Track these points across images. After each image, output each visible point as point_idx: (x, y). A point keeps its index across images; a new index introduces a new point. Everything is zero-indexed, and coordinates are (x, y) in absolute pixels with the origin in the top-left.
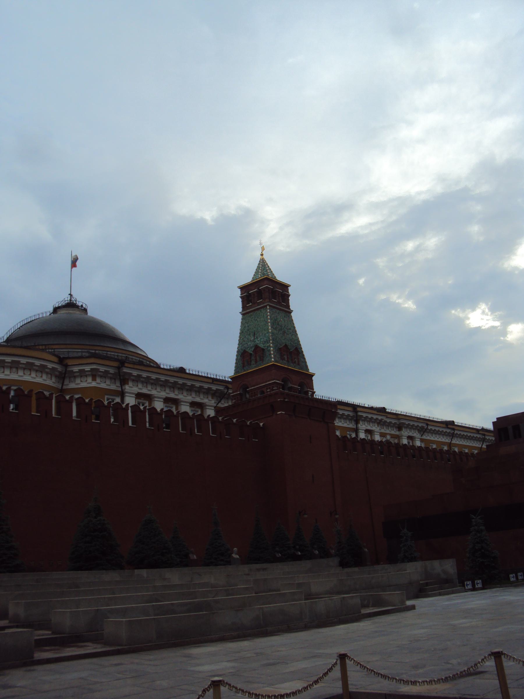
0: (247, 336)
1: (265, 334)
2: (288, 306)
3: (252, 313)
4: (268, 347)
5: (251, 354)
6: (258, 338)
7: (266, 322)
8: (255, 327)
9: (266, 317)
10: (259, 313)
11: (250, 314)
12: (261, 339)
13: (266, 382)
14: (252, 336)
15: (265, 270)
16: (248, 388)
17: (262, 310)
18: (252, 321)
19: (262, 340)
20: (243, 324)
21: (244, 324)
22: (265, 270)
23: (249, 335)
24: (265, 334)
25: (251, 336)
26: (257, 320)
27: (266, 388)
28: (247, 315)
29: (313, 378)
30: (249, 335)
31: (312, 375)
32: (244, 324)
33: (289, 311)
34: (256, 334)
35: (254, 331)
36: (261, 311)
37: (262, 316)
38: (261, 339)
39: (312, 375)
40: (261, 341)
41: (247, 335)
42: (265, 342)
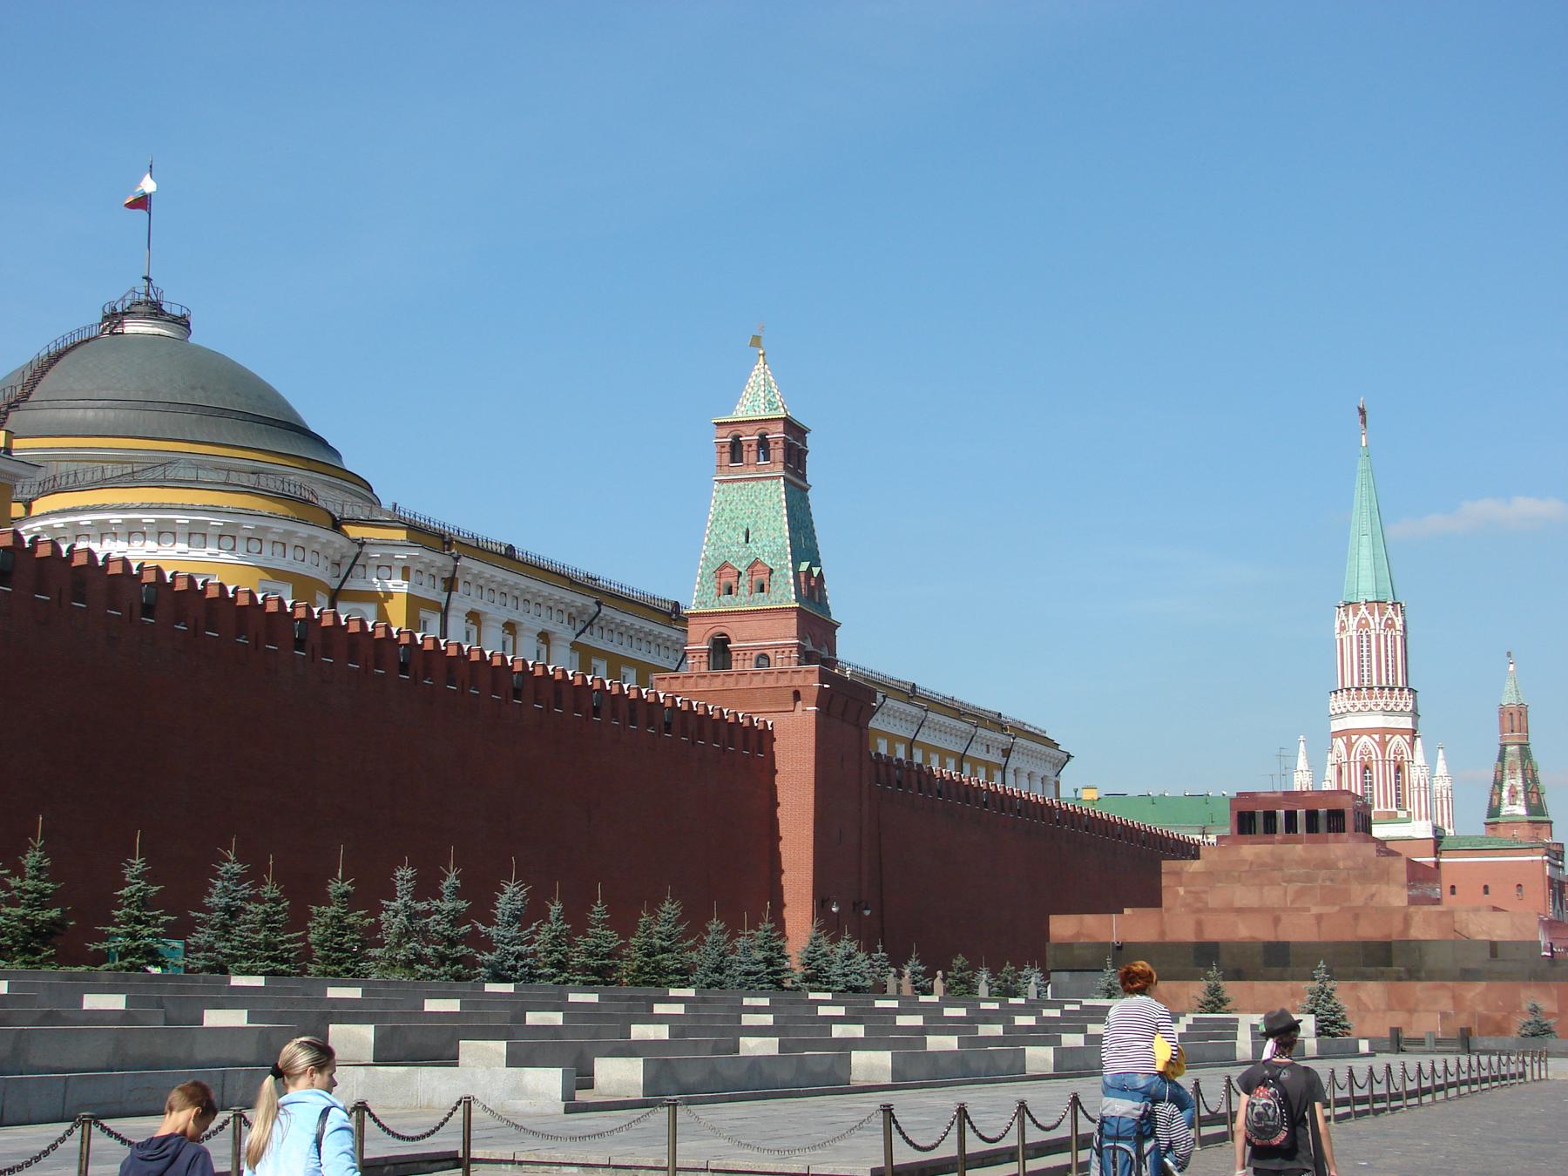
0: (728, 532)
1: (775, 538)
2: (803, 477)
3: (741, 484)
4: (782, 567)
5: (740, 573)
6: (756, 543)
7: (778, 513)
8: (749, 517)
9: (778, 502)
10: (761, 489)
11: (736, 485)
12: (765, 545)
13: (776, 639)
14: (741, 534)
15: (772, 394)
16: (730, 643)
17: (769, 482)
18: (740, 500)
19: (767, 549)
20: (718, 503)
21: (721, 503)
22: (772, 394)
23: (734, 529)
24: (775, 538)
25: (738, 534)
26: (753, 501)
27: (774, 650)
28: (730, 484)
29: (838, 632)
30: (734, 529)
31: (835, 626)
32: (721, 503)
33: (801, 483)
34: (752, 534)
35: (748, 524)
36: (764, 485)
37: (768, 497)
38: (765, 545)
39: (835, 626)
40: (764, 551)
41: (728, 528)
42: (775, 555)
